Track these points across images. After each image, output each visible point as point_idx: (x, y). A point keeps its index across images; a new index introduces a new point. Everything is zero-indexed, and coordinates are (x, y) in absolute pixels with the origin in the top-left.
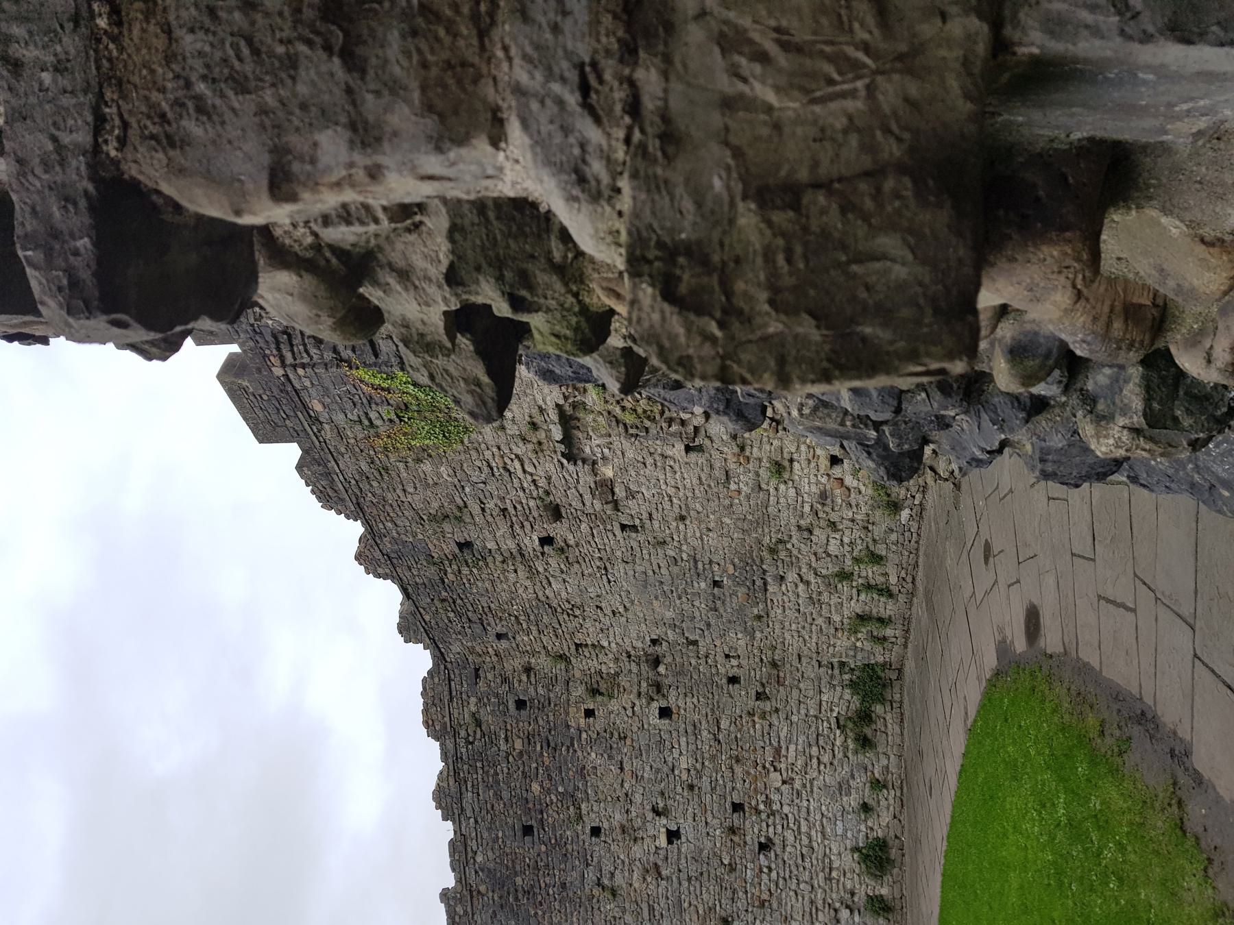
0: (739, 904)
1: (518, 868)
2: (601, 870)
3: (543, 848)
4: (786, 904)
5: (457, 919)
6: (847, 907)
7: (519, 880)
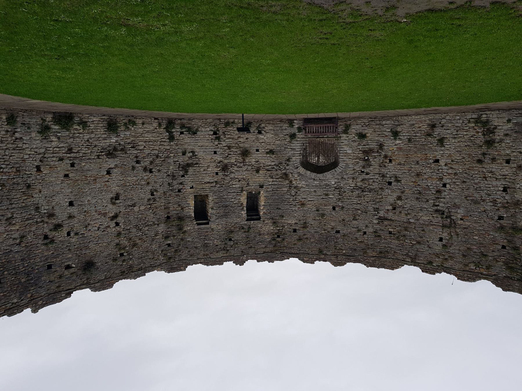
0: (20, 181)
1: (17, 282)
2: (13, 244)
4: (16, 160)
5: (44, 303)
6: (14, 134)
7: (23, 280)
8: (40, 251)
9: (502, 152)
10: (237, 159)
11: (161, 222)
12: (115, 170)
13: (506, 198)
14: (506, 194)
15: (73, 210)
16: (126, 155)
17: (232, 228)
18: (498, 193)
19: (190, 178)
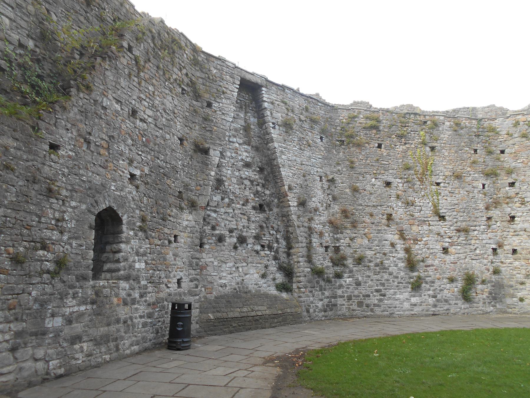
9: (523, 263)
13: (509, 208)
14: (511, 213)
18: (521, 214)
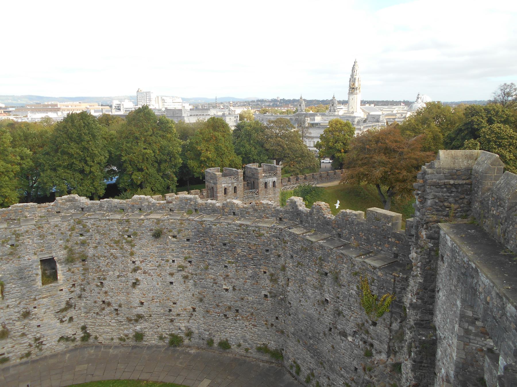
3: (219, 249)
8: (195, 254)
10: (13, 326)
11: (91, 258)
12: (136, 305)
15: (170, 279)
16: (127, 316)
17: (12, 258)
19: (63, 298)
